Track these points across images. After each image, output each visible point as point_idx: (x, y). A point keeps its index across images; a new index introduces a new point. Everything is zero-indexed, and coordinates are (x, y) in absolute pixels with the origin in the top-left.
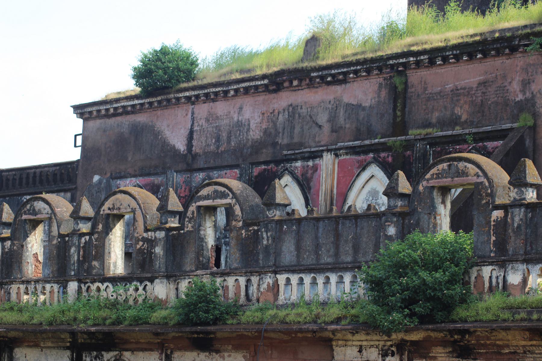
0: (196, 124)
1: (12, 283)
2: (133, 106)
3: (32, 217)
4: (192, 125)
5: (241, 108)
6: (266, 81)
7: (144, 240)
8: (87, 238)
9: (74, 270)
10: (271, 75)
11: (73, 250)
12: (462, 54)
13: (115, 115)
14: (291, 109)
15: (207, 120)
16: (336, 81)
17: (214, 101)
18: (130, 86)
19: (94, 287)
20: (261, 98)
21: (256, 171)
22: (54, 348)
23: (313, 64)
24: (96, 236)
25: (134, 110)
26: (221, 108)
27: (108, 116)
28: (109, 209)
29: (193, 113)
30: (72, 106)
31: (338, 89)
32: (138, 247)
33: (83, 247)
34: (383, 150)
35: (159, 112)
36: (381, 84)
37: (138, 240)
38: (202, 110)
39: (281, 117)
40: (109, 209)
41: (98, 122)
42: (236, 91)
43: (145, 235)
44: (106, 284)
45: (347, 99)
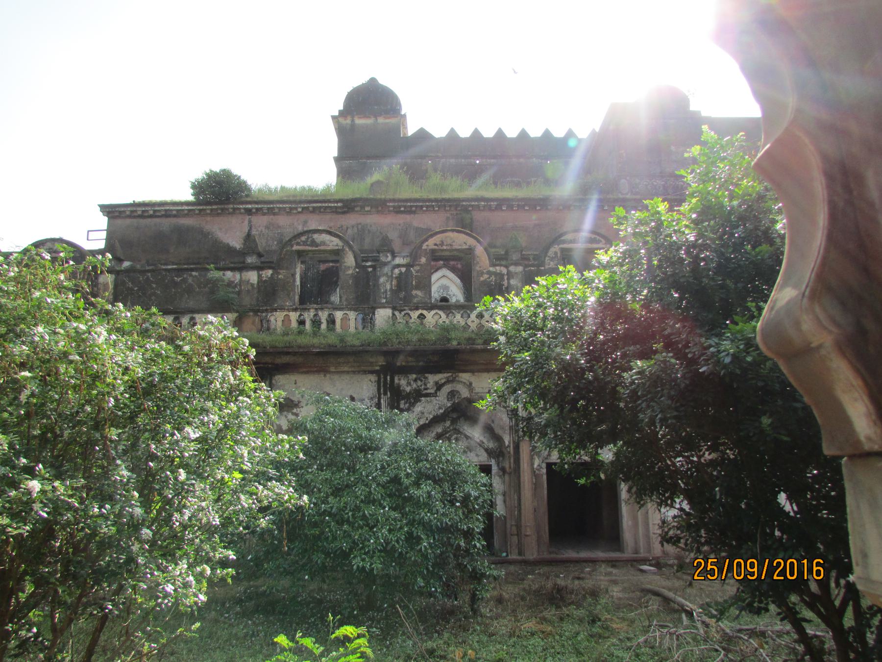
0: (253, 229)
1: (276, 310)
2: (178, 211)
3: (314, 248)
4: (249, 231)
5: (305, 222)
6: (339, 205)
7: (489, 273)
8: (403, 270)
9: (386, 298)
10: (347, 200)
11: (382, 280)
12: (524, 206)
13: (151, 216)
14: (360, 226)
15: (267, 227)
16: (410, 211)
17: (274, 214)
18: (186, 195)
19: (415, 314)
20: (328, 217)
21: (323, 267)
22: (348, 372)
23: (388, 197)
24: (417, 268)
25: (189, 214)
26: (283, 221)
27: (142, 217)
28: (436, 245)
29: (250, 222)
30: (100, 206)
31: (408, 218)
32: (482, 279)
33: (396, 278)
34: (453, 260)
35: (209, 219)
36: (448, 218)
37: (482, 273)
38: (260, 222)
39: (350, 231)
40: (436, 245)
41: (128, 221)
42: (303, 208)
43: (491, 269)
44: (433, 312)
45: (415, 224)
